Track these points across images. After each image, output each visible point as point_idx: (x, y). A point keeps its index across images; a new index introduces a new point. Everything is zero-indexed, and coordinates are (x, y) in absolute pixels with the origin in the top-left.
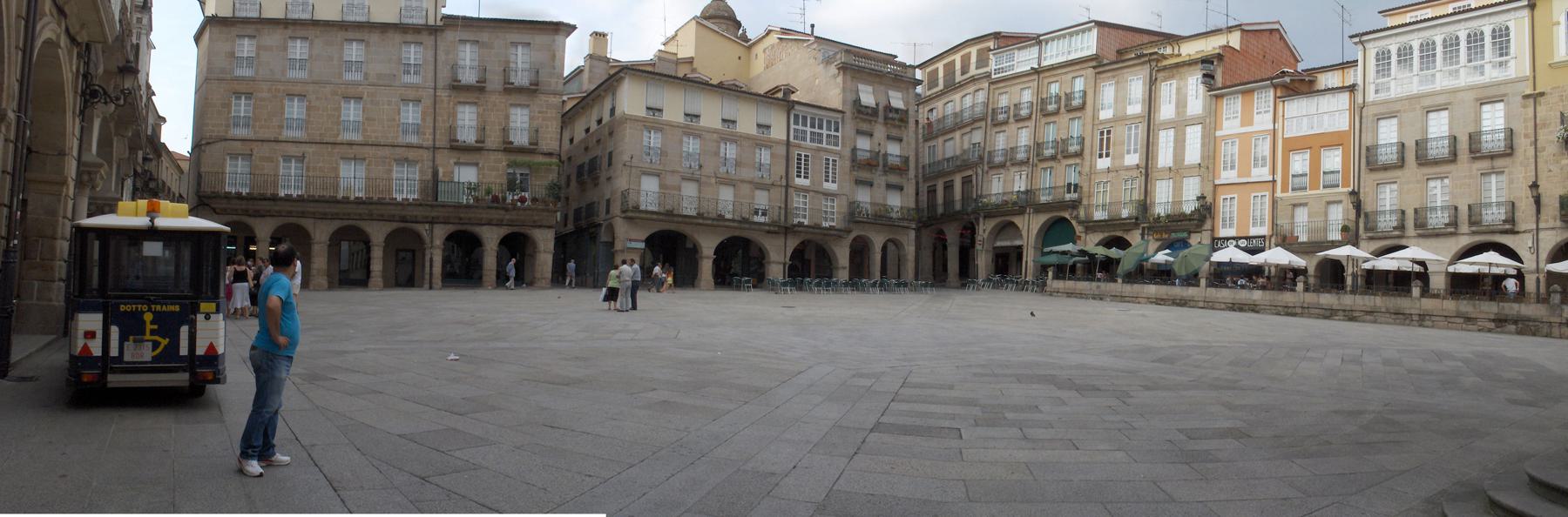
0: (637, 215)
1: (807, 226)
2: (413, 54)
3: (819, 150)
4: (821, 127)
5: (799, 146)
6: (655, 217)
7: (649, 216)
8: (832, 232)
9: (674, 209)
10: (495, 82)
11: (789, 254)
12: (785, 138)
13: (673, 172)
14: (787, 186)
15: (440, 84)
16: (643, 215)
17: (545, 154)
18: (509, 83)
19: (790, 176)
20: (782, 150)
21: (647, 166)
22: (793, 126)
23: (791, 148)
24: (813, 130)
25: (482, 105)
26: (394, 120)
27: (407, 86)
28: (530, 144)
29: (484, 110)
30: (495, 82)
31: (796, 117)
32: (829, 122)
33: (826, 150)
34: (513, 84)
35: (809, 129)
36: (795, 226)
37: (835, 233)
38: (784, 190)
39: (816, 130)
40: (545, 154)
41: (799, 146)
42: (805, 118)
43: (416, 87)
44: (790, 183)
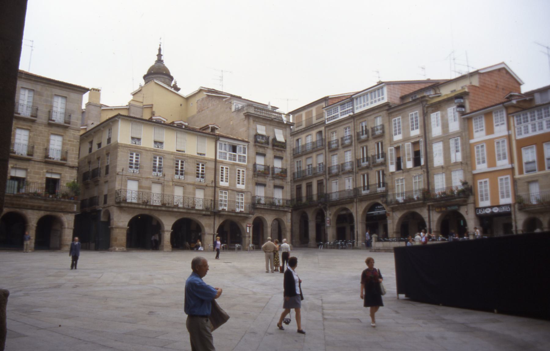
3: (234, 165)
5: (222, 162)
12: (213, 157)
19: (217, 180)
20: (211, 165)
22: (218, 150)
23: (217, 164)
31: (221, 144)
33: (238, 165)
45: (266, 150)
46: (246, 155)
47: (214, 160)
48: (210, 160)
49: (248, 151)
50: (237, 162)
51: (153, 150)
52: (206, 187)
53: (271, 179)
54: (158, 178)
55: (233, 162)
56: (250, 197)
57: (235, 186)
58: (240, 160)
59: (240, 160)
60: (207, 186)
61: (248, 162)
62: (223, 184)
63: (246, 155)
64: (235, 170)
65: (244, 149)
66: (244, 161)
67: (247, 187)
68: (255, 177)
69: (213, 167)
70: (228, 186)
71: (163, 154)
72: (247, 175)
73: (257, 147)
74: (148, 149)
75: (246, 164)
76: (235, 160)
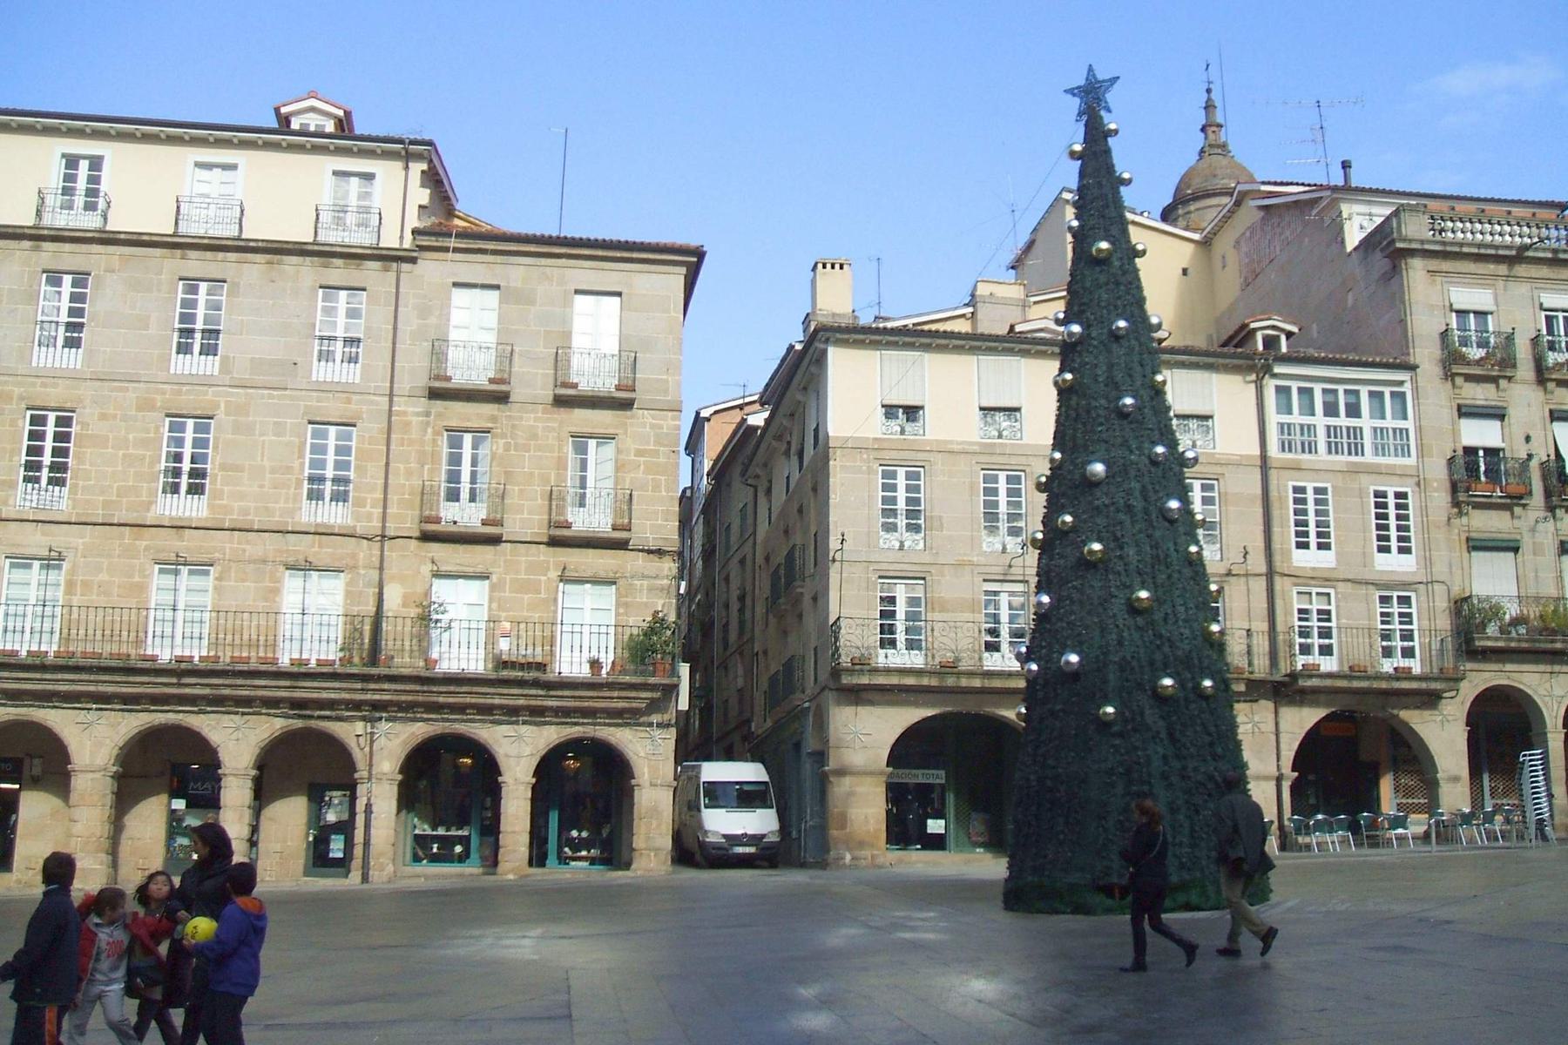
0: (865, 680)
1: (1330, 675)
2: (338, 315)
3: (1355, 470)
4: (1353, 411)
5: (1296, 468)
6: (910, 681)
7: (894, 680)
8: (1405, 685)
9: (957, 659)
10: (532, 383)
11: (1289, 754)
12: (1257, 452)
13: (960, 565)
14: (1270, 574)
15: (404, 384)
16: (881, 680)
17: (650, 552)
18: (565, 385)
19: (1276, 545)
20: (1251, 483)
21: (891, 557)
22: (1273, 418)
23: (1273, 474)
24: (1332, 421)
25: (503, 436)
26: (289, 469)
27: (323, 389)
28: (615, 528)
29: (507, 448)
30: (532, 383)
31: (1283, 391)
32: (1376, 396)
33: (1374, 471)
34: (575, 386)
35: (1320, 421)
36: (1293, 676)
37: (1414, 685)
38: (1260, 586)
39: (1343, 421)
40: (650, 552)
41: (1296, 468)
42: (1306, 393)
43: (346, 391)
44: (1279, 565)
45: (1504, 390)
46: (1409, 424)
47: (1259, 463)
48: (1239, 463)
49: (1416, 405)
50: (1369, 457)
51: (976, 448)
52: (1227, 579)
53: (1542, 514)
54: (1006, 560)
55: (1344, 458)
56: (1442, 603)
57: (1366, 561)
58: (1380, 449)
59: (1380, 449)
60: (1229, 574)
61: (1421, 454)
62: (1309, 559)
63: (1409, 424)
64: (1362, 493)
65: (1399, 397)
66: (1404, 451)
67: (1427, 562)
68: (1460, 514)
69: (1259, 491)
70: (1333, 565)
71: (1023, 460)
72: (1424, 511)
73: (1459, 381)
74: (956, 447)
75: (1411, 461)
76: (1357, 449)
